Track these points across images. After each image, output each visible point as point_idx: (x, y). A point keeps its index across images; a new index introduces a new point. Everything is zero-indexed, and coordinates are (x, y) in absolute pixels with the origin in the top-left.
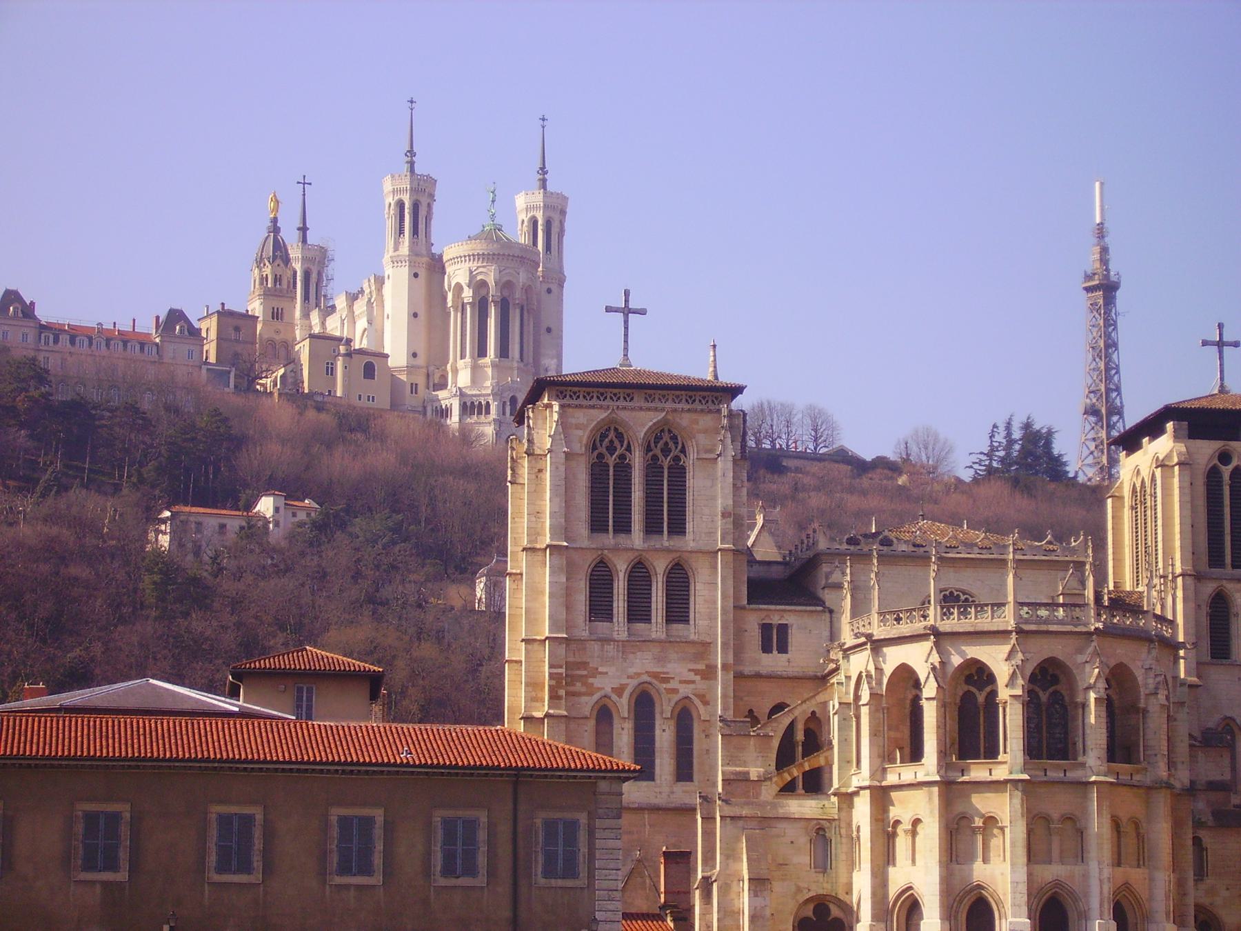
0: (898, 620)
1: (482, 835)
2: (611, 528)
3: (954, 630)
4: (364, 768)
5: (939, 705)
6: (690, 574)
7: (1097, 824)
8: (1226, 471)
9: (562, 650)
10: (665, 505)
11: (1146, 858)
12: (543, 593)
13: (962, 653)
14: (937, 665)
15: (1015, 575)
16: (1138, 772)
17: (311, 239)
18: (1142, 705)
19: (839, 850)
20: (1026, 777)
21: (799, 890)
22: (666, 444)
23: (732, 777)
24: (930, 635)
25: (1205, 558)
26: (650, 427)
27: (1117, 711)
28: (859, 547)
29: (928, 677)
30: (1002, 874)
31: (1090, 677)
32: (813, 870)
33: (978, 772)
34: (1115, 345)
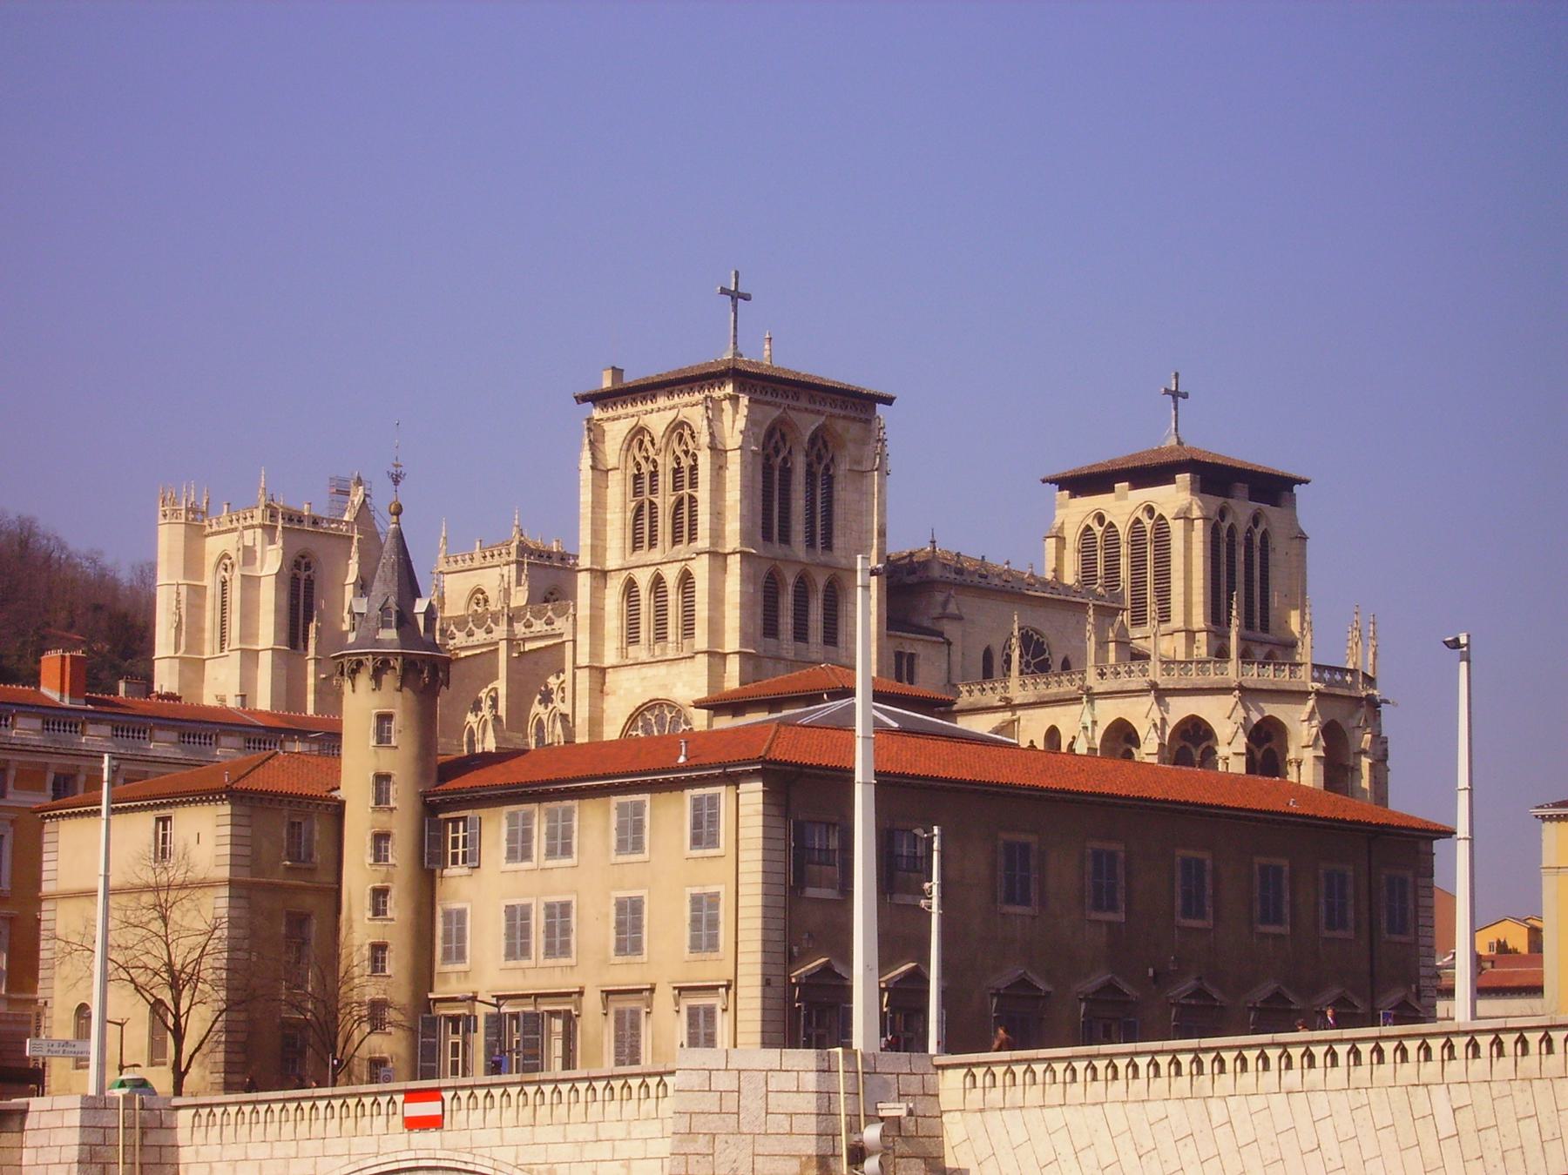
8: (1225, 525)
13: (1261, 711)
24: (1234, 689)
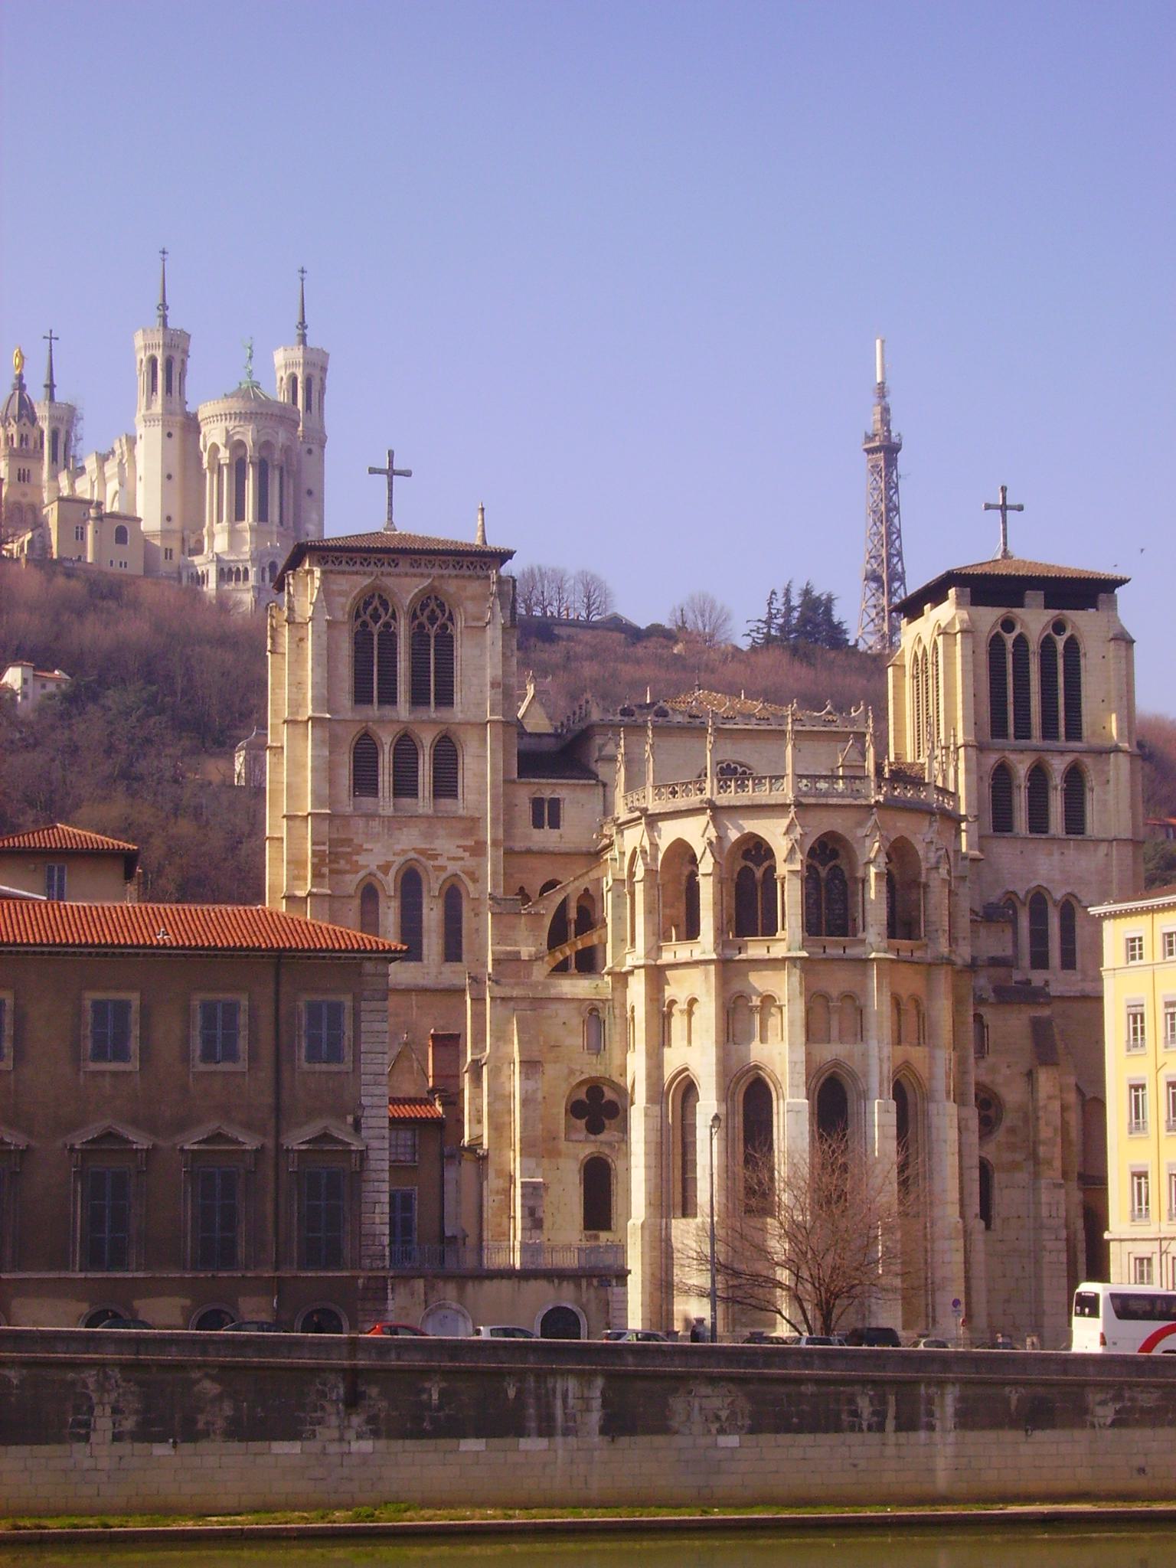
0: (674, 793)
1: (243, 1019)
2: (375, 699)
3: (731, 804)
4: (119, 950)
5: (716, 881)
6: (458, 747)
7: (877, 1002)
8: (1010, 639)
9: (325, 826)
10: (432, 675)
11: (926, 1037)
12: (305, 766)
13: (739, 828)
14: (714, 840)
15: (794, 746)
16: (919, 948)
17: (59, 397)
18: (923, 880)
19: (613, 1032)
20: (805, 954)
21: (572, 1072)
22: (433, 611)
23: (502, 957)
24: (706, 809)
25: (987, 729)
26: (416, 594)
27: (897, 886)
28: (633, 718)
29: (704, 853)
30: (780, 1054)
31: (870, 852)
32: (586, 1051)
33: (756, 949)
34: (897, 509)
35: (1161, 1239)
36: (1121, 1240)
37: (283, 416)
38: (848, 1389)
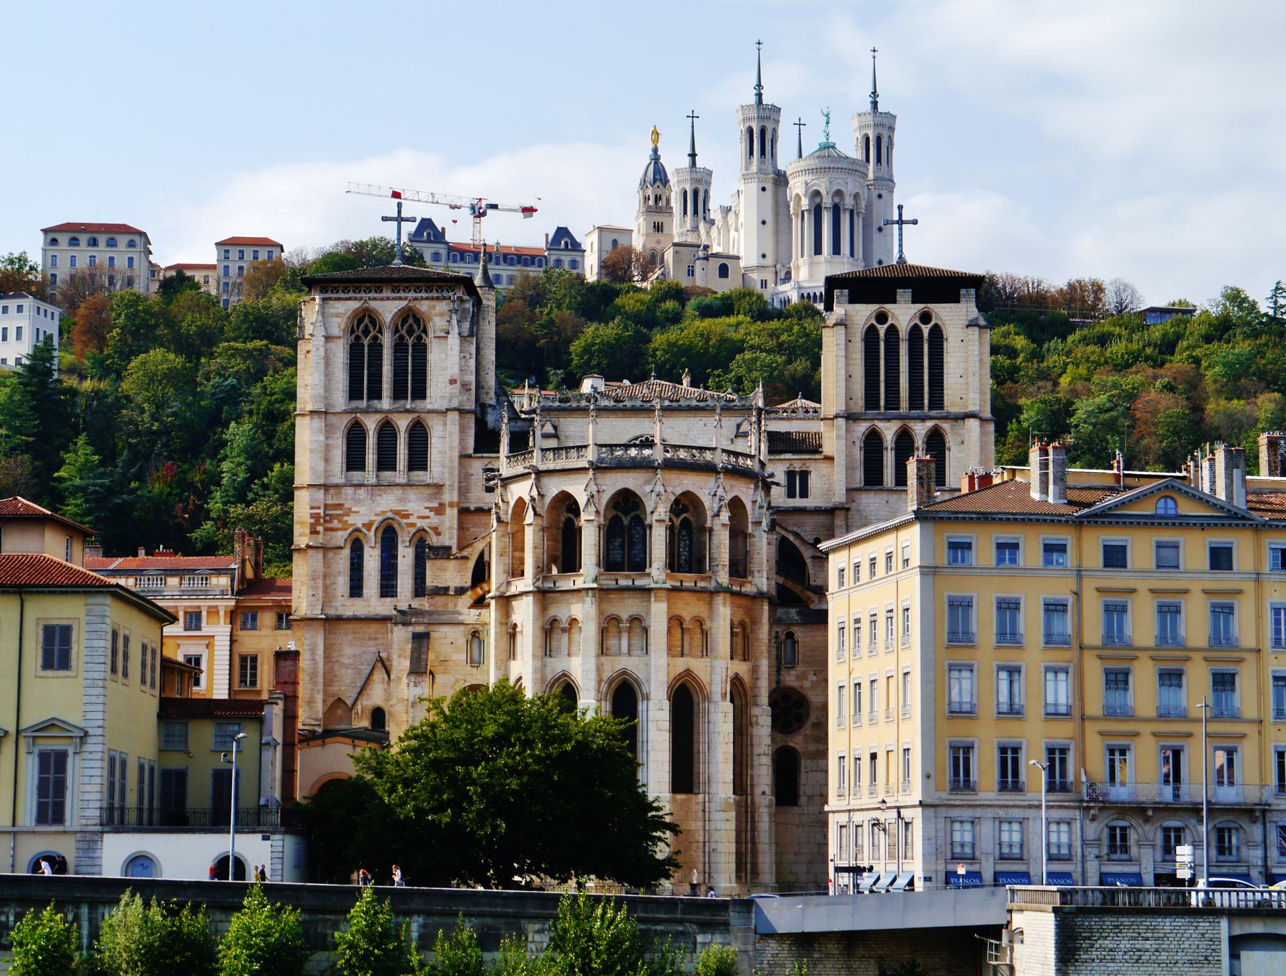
2: (365, 396)
5: (537, 529)
8: (882, 329)
14: (536, 497)
16: (703, 579)
18: (708, 524)
20: (595, 585)
21: (457, 681)
22: (411, 326)
24: (530, 474)
27: (694, 531)
33: (566, 584)
35: (849, 811)
36: (833, 812)
37: (853, 168)
38: (333, 917)
